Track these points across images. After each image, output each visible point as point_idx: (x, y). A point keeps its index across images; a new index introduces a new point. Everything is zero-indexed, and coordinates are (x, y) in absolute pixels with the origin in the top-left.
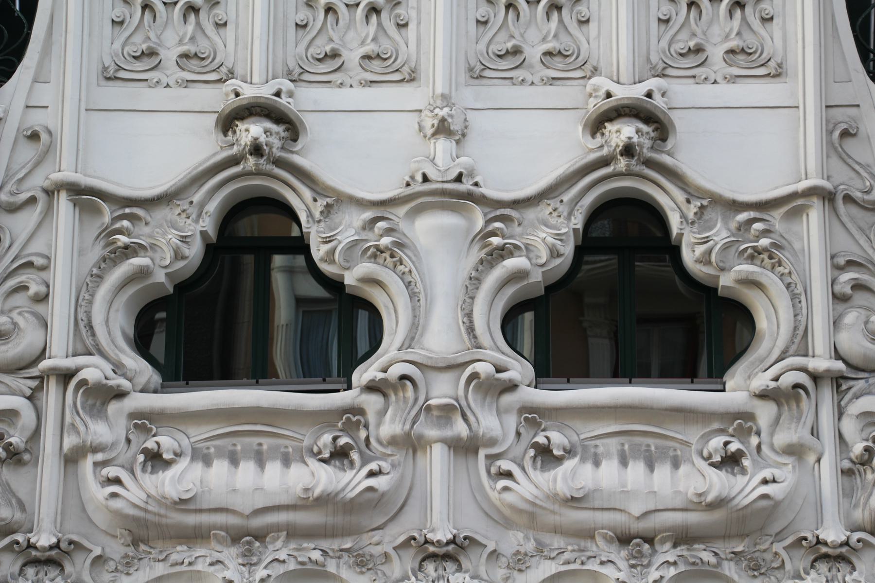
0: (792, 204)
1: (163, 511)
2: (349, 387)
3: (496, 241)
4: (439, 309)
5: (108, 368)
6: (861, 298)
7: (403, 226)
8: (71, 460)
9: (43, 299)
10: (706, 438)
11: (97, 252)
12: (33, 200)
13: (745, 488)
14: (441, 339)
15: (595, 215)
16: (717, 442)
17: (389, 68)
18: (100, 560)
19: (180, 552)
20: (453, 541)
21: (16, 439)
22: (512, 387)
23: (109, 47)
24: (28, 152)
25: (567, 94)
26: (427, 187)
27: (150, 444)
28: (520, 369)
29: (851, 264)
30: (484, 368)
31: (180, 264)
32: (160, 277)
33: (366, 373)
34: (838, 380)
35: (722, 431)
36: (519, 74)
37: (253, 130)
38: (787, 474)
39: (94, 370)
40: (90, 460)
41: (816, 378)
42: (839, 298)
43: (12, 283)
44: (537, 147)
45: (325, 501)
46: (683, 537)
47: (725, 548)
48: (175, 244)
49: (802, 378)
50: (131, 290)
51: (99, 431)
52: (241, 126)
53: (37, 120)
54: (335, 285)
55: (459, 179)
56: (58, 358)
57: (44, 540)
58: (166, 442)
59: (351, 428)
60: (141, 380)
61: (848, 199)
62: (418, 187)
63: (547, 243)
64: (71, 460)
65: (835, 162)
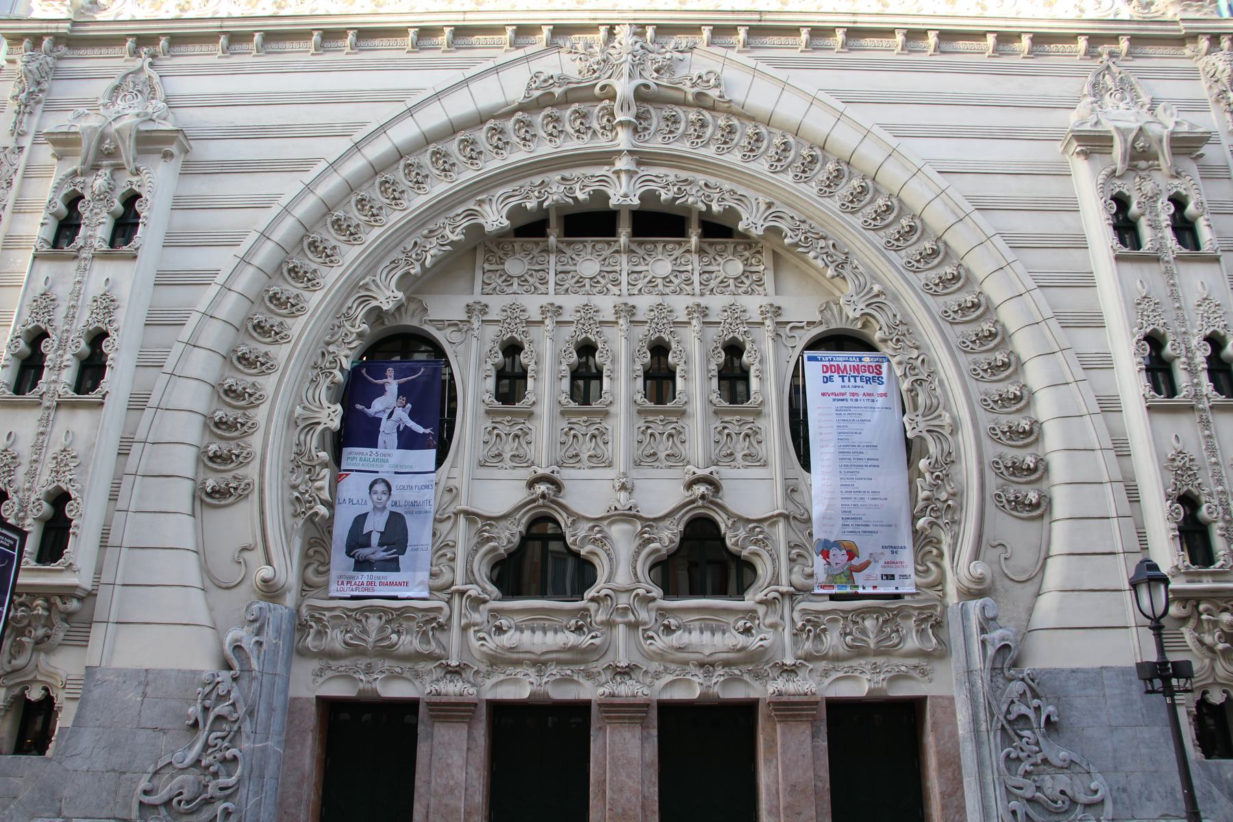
0: (772, 520)
3: (646, 536)
4: (621, 566)
6: (800, 560)
7: (606, 529)
8: (465, 629)
9: (453, 560)
10: (737, 621)
12: (449, 517)
13: (753, 642)
14: (622, 578)
15: (689, 525)
16: (741, 623)
17: (600, 461)
18: (477, 672)
19: (510, 670)
22: (654, 599)
23: (482, 452)
24: (448, 497)
25: (676, 473)
27: (497, 623)
28: (657, 592)
30: (641, 592)
32: (502, 551)
34: (791, 595)
35: (743, 618)
36: (656, 464)
37: (542, 488)
38: (770, 636)
39: (474, 591)
40: (472, 629)
41: (782, 594)
42: (792, 560)
44: (663, 494)
45: (573, 649)
46: (727, 664)
47: (744, 668)
48: (507, 536)
49: (777, 595)
50: (489, 556)
51: (476, 617)
52: (537, 486)
53: (452, 483)
54: (576, 555)
55: (630, 509)
57: (454, 663)
58: (504, 622)
59: (583, 617)
60: (494, 596)
61: (794, 518)
63: (668, 536)
64: (465, 629)
65: (789, 502)
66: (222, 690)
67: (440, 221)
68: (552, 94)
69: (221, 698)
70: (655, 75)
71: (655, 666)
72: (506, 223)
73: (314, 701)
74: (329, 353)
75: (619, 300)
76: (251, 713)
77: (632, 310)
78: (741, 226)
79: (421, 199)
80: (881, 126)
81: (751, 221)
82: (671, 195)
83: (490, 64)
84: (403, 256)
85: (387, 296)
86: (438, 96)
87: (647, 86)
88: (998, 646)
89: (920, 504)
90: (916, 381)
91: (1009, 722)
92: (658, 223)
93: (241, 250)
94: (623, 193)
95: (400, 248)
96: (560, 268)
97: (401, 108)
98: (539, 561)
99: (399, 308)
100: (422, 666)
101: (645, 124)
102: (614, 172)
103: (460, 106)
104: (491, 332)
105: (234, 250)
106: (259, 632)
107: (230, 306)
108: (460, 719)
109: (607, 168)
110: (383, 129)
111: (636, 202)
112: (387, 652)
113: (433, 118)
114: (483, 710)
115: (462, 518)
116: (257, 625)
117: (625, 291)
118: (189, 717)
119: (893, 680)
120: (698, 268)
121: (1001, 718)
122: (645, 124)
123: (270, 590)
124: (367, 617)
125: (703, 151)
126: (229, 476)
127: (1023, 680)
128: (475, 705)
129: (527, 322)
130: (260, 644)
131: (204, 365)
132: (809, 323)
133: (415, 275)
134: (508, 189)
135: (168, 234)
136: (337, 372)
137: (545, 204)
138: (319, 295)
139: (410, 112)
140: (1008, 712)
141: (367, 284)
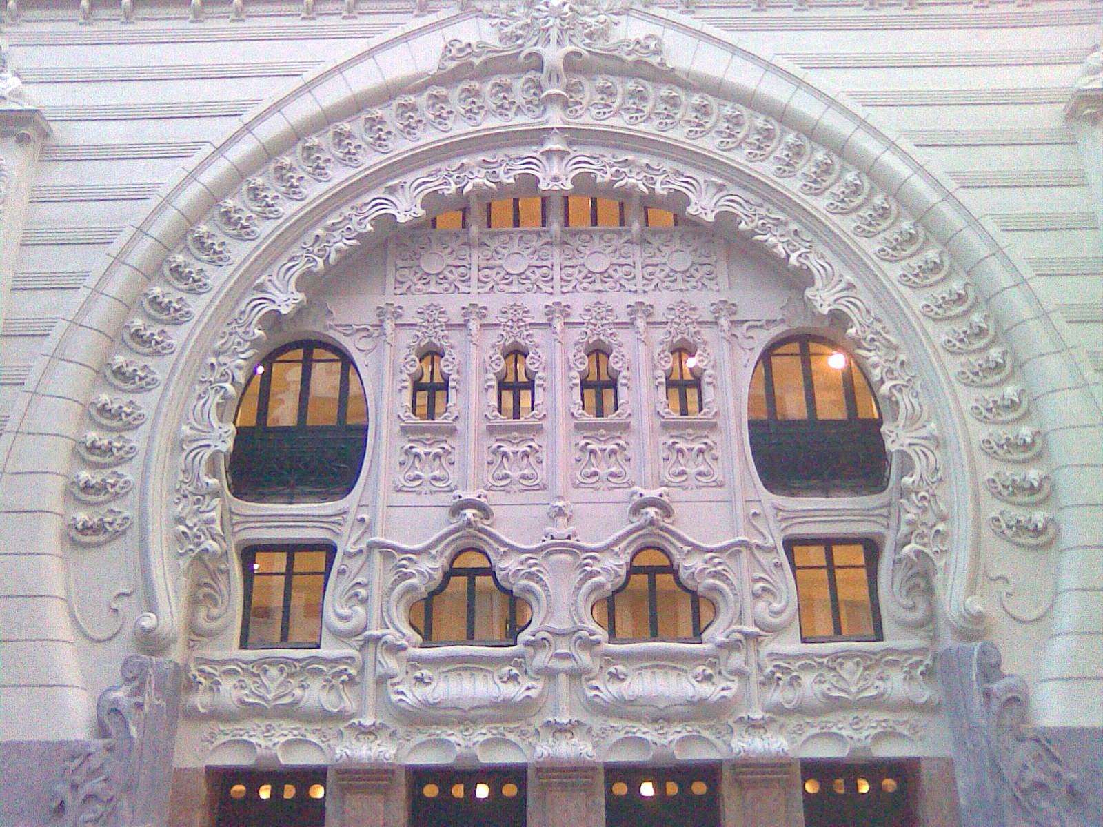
1: (424, 708)
4: (561, 605)
5: (398, 634)
11: (392, 578)
12: (361, 551)
14: (561, 622)
16: (700, 669)
20: (570, 722)
21: (352, 671)
22: (598, 643)
26: (554, 541)
29: (761, 579)
30: (584, 633)
33: (525, 636)
37: (469, 513)
39: (391, 636)
40: (390, 681)
41: (747, 636)
43: (350, 593)
45: (507, 703)
49: (739, 636)
55: (569, 538)
56: (374, 632)
59: (518, 665)
61: (758, 546)
62: (549, 541)
64: (381, 681)
66: (95, 762)
67: (346, 211)
68: (471, 64)
69: (93, 773)
70: (588, 41)
71: (597, 723)
74: (220, 365)
76: (127, 789)
77: (566, 311)
78: (691, 210)
79: (323, 187)
80: (851, 94)
82: (608, 177)
83: (398, 32)
84: (304, 253)
85: (286, 300)
86: (339, 69)
87: (578, 54)
88: (1004, 699)
89: (904, 529)
90: (894, 386)
91: (1023, 792)
93: (114, 249)
96: (483, 264)
99: (300, 311)
100: (330, 728)
101: (577, 97)
102: (542, 153)
103: (363, 79)
104: (407, 337)
105: (109, 248)
106: (138, 691)
107: (102, 312)
108: (376, 790)
109: (535, 148)
110: (277, 107)
112: (292, 712)
113: (332, 94)
114: (402, 779)
115: (377, 556)
116: (136, 683)
117: (557, 289)
118: (54, 797)
119: (878, 738)
120: (639, 260)
121: (1011, 783)
122: (577, 97)
123: (150, 642)
124: (266, 671)
125: (642, 127)
126: (103, 510)
127: (1037, 741)
128: (393, 772)
129: (447, 325)
130: (140, 706)
131: (70, 380)
132: (768, 322)
134: (422, 174)
135: (26, 231)
136: (228, 386)
139: (307, 87)
140: (1020, 778)
141: (262, 284)
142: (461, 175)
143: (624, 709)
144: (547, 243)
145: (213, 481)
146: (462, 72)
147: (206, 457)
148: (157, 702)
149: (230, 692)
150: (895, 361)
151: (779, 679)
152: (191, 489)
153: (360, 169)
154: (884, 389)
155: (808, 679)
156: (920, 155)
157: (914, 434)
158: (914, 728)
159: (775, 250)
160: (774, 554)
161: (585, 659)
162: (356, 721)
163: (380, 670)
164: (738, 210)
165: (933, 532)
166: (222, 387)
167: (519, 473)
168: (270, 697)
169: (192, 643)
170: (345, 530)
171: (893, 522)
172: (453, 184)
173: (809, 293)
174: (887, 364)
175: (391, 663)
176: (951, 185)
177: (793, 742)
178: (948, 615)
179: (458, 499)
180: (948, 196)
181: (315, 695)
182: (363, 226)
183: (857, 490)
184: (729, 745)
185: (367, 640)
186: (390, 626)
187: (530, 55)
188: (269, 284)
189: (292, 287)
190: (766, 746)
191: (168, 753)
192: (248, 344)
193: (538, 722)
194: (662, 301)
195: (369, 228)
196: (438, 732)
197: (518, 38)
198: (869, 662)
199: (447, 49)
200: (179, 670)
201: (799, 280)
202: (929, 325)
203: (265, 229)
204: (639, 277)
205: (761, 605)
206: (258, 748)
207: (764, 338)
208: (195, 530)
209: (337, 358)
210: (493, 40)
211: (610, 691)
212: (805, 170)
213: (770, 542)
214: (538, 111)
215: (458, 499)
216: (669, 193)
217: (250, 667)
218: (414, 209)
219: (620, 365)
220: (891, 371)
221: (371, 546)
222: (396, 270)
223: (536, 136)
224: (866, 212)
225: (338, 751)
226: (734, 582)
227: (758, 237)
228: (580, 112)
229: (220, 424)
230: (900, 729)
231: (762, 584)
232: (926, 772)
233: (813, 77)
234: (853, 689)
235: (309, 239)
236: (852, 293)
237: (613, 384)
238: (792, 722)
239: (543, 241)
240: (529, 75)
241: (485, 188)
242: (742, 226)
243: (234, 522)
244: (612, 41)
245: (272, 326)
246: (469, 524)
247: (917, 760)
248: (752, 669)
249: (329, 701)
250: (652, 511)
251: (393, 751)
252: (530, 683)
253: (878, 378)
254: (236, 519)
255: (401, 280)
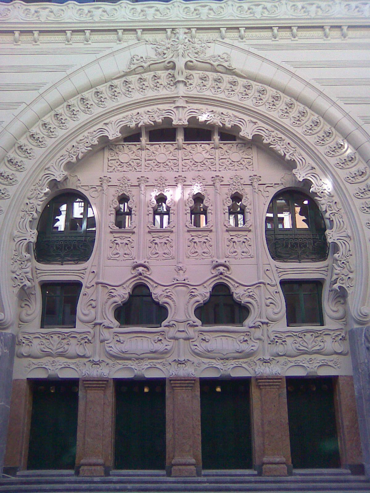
2: (161, 327)
4: (181, 309)
7: (173, 291)
11: (107, 297)
14: (181, 317)
15: (214, 288)
21: (90, 338)
24: (93, 274)
26: (178, 282)
28: (199, 322)
30: (191, 322)
31: (124, 299)
32: (120, 302)
33: (164, 323)
34: (267, 323)
37: (141, 269)
39: (106, 323)
41: (263, 323)
43: (89, 304)
54: (157, 304)
55: (184, 280)
60: (116, 325)
62: (175, 282)
67: (86, 134)
71: (196, 359)
72: (120, 135)
73: (26, 381)
74: (30, 203)
75: (177, 175)
78: (241, 134)
79: (76, 123)
81: (247, 132)
84: (67, 153)
85: (59, 174)
89: (335, 277)
92: (198, 133)
94: (180, 118)
95: (65, 149)
96: (147, 158)
97: (64, 74)
98: (140, 308)
99: (66, 179)
101: (191, 82)
103: (95, 73)
109: (171, 105)
110: (54, 86)
111: (186, 123)
114: (111, 383)
117: (180, 170)
122: (191, 82)
128: (107, 381)
133: (73, 163)
136: (34, 213)
137: (139, 125)
138: (24, 173)
139: (68, 77)
141: (49, 168)
142: (138, 118)
143: (208, 354)
144: (176, 149)
145: (28, 256)
146: (139, 69)
147: (25, 244)
148: (5, 351)
149: (36, 347)
150: (332, 202)
151: (277, 342)
152: (18, 258)
153: (93, 115)
154: (327, 215)
155: (289, 341)
156: (347, 108)
157: (338, 235)
158: (336, 363)
159: (279, 152)
160: (275, 288)
161: (191, 332)
162: (91, 359)
163: (102, 338)
164: (262, 133)
165: (347, 277)
166: (31, 214)
167: (163, 252)
168: (54, 348)
169: (20, 325)
170: (86, 276)
171: (329, 273)
172: (134, 122)
173: (294, 171)
174: (329, 203)
175: (106, 334)
176: (360, 122)
177: (282, 368)
178: (353, 315)
179: (135, 263)
180: (359, 127)
181: (74, 348)
182: (93, 141)
183: (314, 260)
184: (255, 370)
185: (96, 324)
186: (106, 318)
187: (169, 62)
188: (51, 167)
189: (62, 169)
190: (271, 371)
191: (10, 373)
192: (43, 194)
193: (171, 359)
194: (227, 175)
195: (96, 143)
196: (127, 364)
197: (164, 54)
198: (316, 334)
199: (132, 59)
200: (14, 337)
201: (290, 165)
202: (348, 185)
203: (49, 142)
204: (217, 164)
205: (270, 310)
206: (49, 370)
207: (273, 191)
208: (20, 276)
209: (82, 200)
210: (152, 54)
211: (202, 347)
212: (293, 115)
213: (274, 283)
214: (173, 88)
215: (135, 263)
216: (232, 126)
217: (45, 335)
218: (117, 134)
219: (208, 204)
220: (330, 206)
221: (97, 283)
222: (108, 161)
223: (171, 100)
224: (321, 134)
225: (84, 372)
226: (257, 299)
227: (271, 146)
228: (192, 89)
229: (31, 230)
230: (330, 364)
231: (270, 301)
232: (341, 382)
233: (298, 72)
234: (310, 347)
235: (69, 146)
236: (313, 171)
237: (205, 212)
238: (282, 360)
239: (175, 148)
240: (170, 71)
241: (148, 124)
242: (265, 141)
243: (37, 273)
244: (207, 55)
245: (53, 187)
246: (140, 274)
247: (337, 377)
248: (265, 338)
249: (80, 351)
250: (221, 269)
251: (108, 372)
252: (167, 343)
253: (324, 210)
254: (38, 271)
255: (111, 166)
